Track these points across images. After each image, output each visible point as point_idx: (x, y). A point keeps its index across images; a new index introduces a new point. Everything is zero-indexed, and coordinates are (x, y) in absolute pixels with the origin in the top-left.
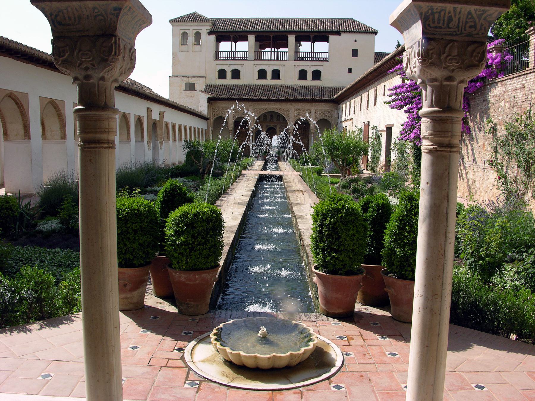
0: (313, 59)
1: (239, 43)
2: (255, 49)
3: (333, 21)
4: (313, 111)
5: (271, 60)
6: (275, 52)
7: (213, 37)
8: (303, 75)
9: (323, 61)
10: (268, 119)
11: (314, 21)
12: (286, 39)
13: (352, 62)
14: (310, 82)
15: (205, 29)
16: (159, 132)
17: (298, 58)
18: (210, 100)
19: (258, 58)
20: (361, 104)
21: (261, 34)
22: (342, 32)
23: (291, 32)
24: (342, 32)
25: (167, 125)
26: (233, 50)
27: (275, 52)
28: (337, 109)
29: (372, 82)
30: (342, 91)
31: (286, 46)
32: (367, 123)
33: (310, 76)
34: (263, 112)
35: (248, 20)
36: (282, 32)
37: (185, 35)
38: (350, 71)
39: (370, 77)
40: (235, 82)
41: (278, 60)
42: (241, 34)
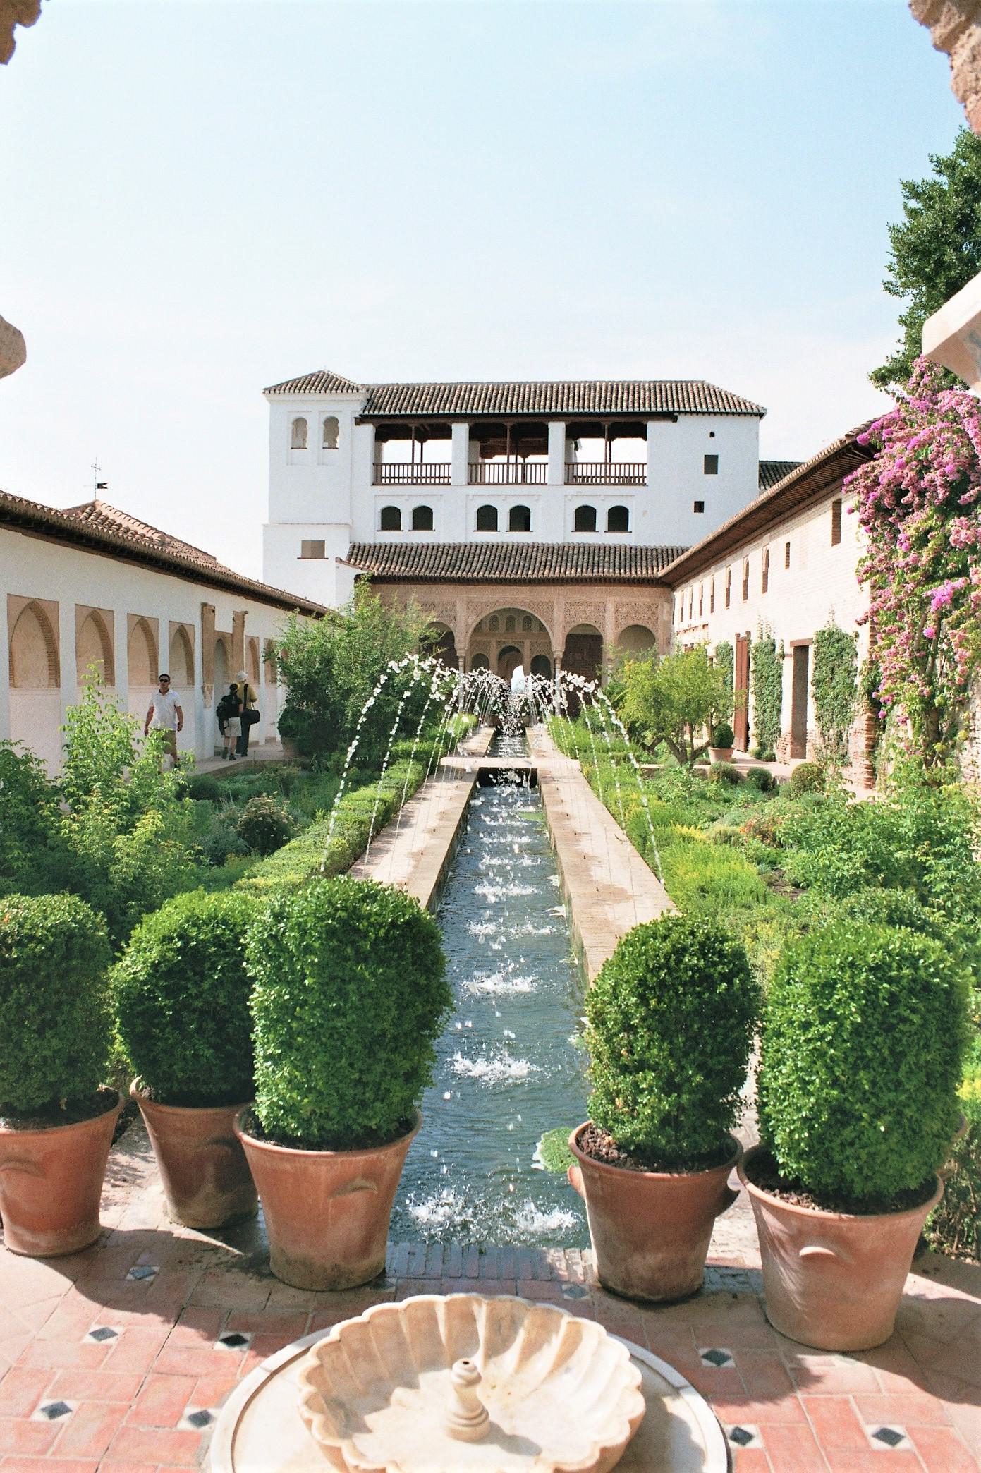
0: (610, 481)
1: (430, 444)
2: (470, 456)
3: (657, 388)
4: (611, 608)
5: (508, 483)
6: (517, 464)
8: (585, 518)
9: (635, 484)
10: (502, 628)
11: (612, 388)
12: (544, 433)
13: (707, 487)
14: (601, 536)
16: (232, 662)
17: (572, 477)
20: (728, 590)
21: (484, 420)
25: (253, 644)
26: (417, 460)
27: (517, 464)
28: (671, 601)
29: (756, 533)
30: (682, 557)
31: (543, 449)
32: (743, 635)
34: (489, 610)
36: (534, 415)
38: (699, 507)
39: (749, 524)
40: (422, 538)
41: (524, 483)
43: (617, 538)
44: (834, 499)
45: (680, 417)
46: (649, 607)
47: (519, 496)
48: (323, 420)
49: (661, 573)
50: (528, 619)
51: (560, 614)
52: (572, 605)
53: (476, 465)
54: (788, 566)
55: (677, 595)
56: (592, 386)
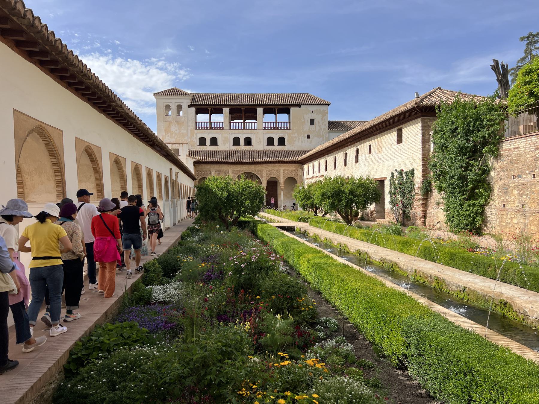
0: (276, 128)
3: (293, 96)
4: (282, 171)
8: (270, 141)
11: (278, 96)
12: (255, 112)
14: (276, 147)
15: (185, 102)
17: (264, 128)
18: (196, 163)
21: (234, 107)
23: (260, 106)
33: (276, 142)
37: (168, 107)
38: (308, 137)
42: (217, 107)
43: (281, 148)
44: (397, 128)
51: (265, 174)
54: (370, 152)
55: (306, 167)
56: (270, 95)
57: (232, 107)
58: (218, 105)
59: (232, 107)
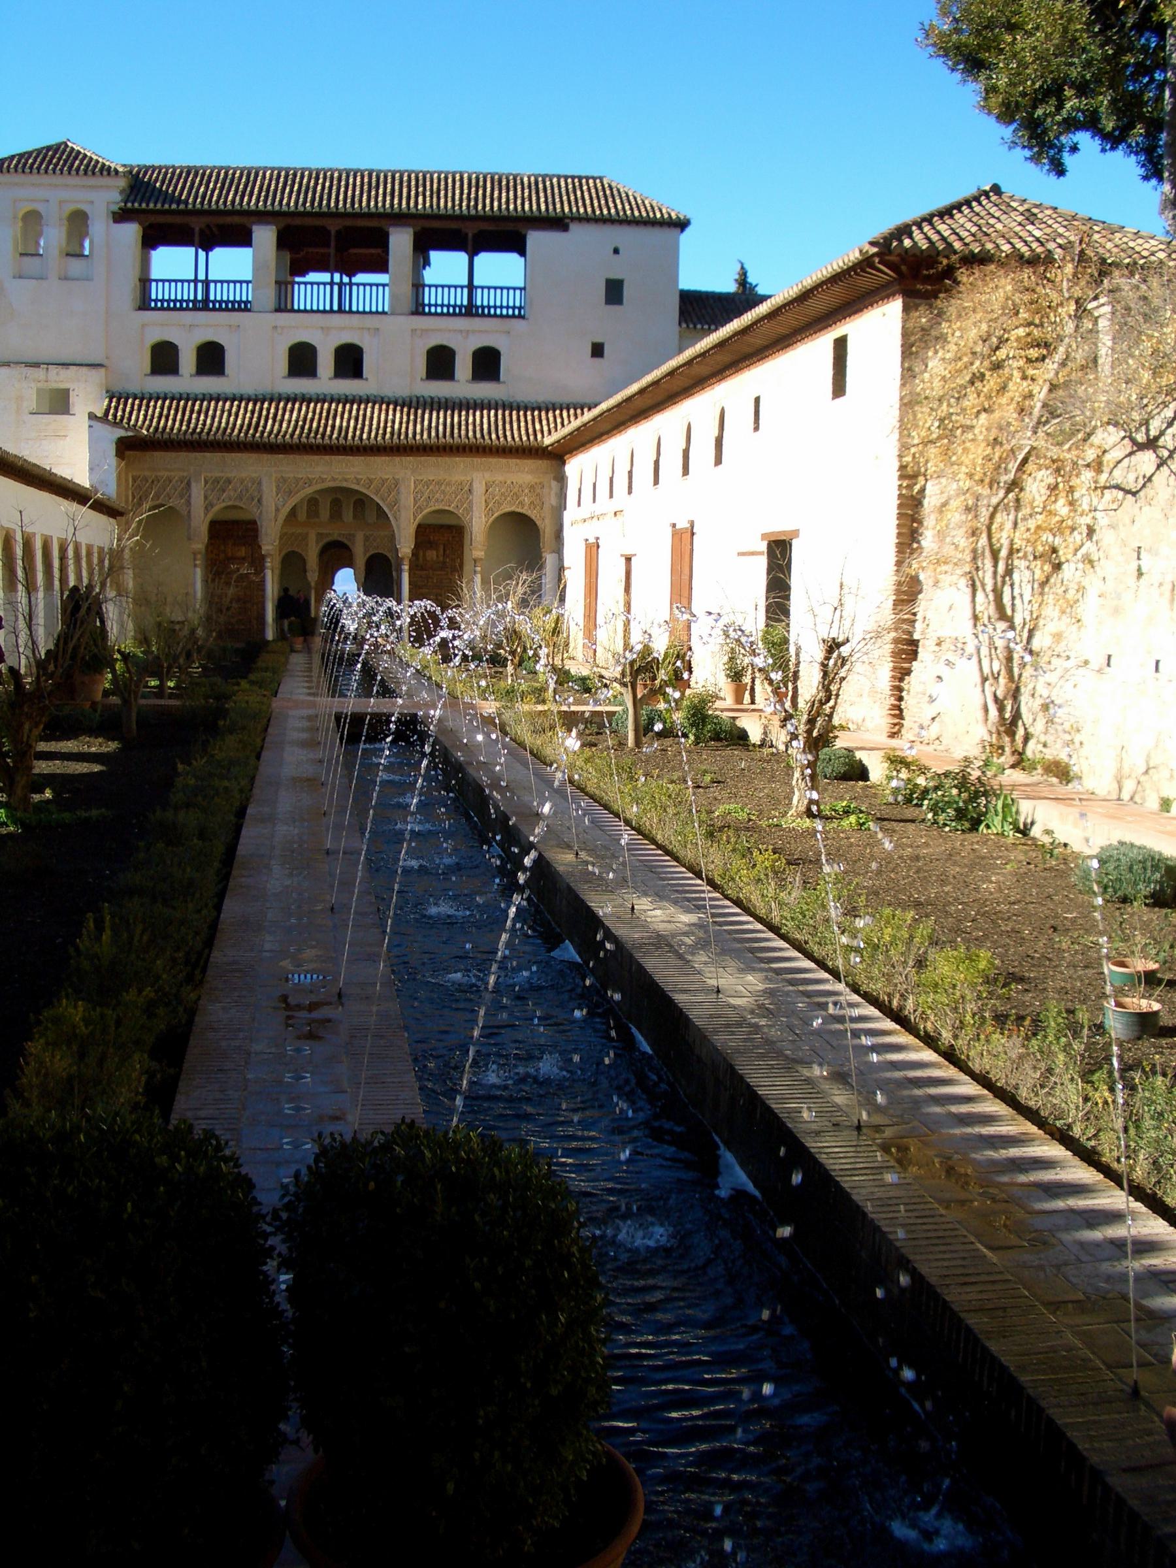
0: (470, 310)
1: (220, 255)
3: (539, 183)
5: (332, 311)
7: (131, 231)
10: (325, 513)
11: (478, 182)
17: (419, 309)
18: (127, 447)
19: (283, 305)
21: (297, 221)
22: (573, 219)
23: (401, 218)
24: (573, 219)
26: (201, 276)
27: (341, 285)
28: (562, 479)
31: (381, 266)
32: (682, 524)
33: (463, 366)
35: (252, 174)
37: (32, 220)
38: (598, 350)
41: (351, 312)
45: (573, 227)
46: (532, 488)
47: (345, 332)
48: (66, 214)
49: (548, 441)
50: (361, 503)
52: (428, 484)
53: (286, 283)
57: (289, 221)
58: (233, 213)
59: (283, 222)
